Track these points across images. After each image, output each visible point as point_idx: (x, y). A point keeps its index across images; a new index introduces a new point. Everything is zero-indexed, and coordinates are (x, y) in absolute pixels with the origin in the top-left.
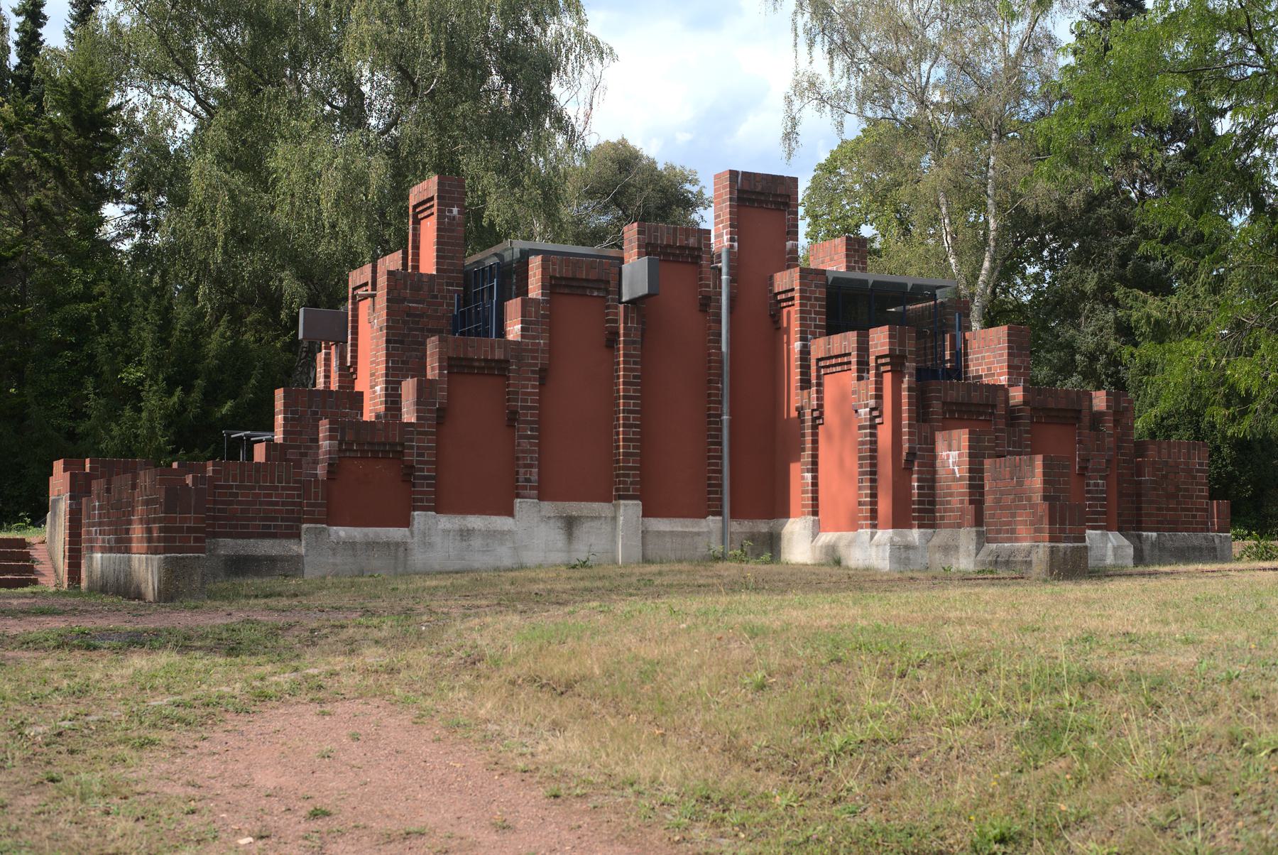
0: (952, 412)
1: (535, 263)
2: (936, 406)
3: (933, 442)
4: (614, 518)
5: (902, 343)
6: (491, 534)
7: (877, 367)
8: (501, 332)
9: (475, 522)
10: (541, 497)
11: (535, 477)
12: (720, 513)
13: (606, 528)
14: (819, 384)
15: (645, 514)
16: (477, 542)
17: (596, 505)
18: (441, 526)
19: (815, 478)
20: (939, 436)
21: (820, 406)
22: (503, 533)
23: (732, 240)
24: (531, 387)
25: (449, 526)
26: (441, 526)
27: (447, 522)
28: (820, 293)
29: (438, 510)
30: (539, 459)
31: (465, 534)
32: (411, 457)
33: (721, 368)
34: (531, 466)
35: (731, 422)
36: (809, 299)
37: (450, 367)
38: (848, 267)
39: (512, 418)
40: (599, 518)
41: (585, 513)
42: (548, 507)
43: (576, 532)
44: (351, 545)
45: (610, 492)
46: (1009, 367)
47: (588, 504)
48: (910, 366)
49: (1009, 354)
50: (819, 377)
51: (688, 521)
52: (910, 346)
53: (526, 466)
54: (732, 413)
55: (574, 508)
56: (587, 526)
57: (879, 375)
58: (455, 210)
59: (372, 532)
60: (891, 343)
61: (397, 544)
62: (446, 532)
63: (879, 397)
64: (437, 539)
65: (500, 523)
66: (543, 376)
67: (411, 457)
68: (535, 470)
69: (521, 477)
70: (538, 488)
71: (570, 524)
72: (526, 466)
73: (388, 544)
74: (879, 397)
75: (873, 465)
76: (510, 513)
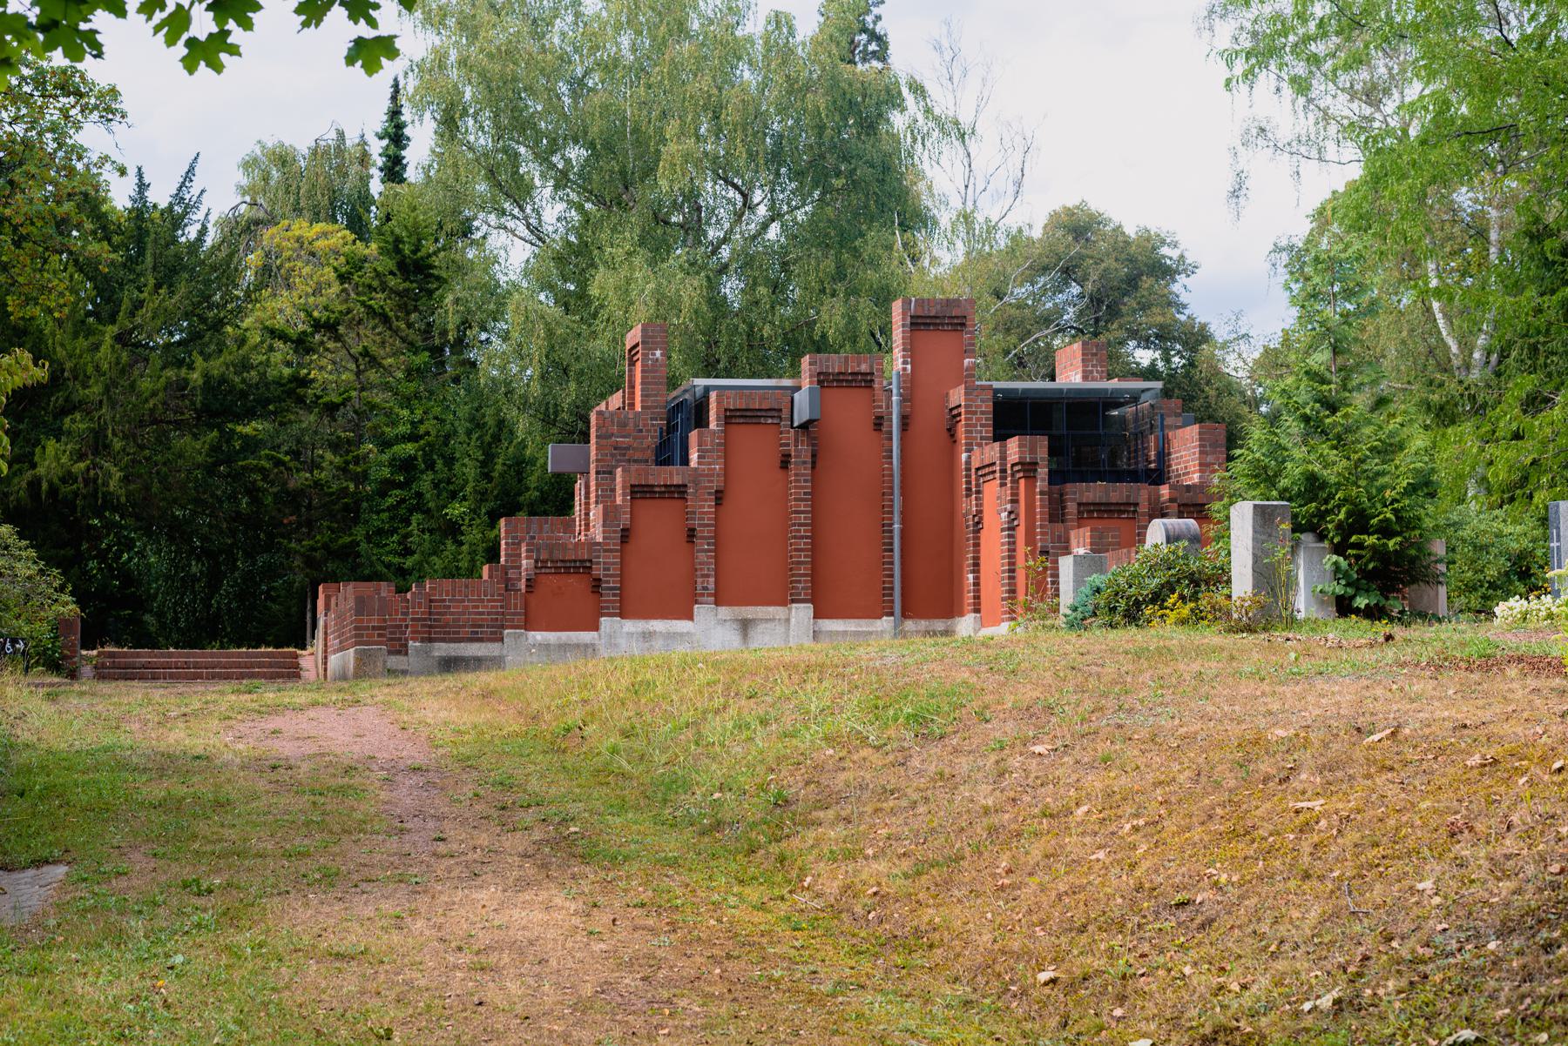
0: (1090, 512)
1: (713, 396)
2: (1072, 507)
3: (1068, 541)
4: (788, 620)
5: (1033, 451)
6: (670, 636)
7: (1013, 475)
8: (685, 461)
9: (658, 625)
10: (717, 603)
11: (712, 586)
12: (892, 614)
13: (780, 629)
14: (978, 492)
15: (818, 615)
16: (658, 643)
17: (771, 609)
18: (625, 629)
19: (977, 578)
20: (1073, 533)
21: (979, 512)
22: (681, 635)
23: (905, 363)
24: (708, 506)
25: (633, 629)
26: (625, 629)
27: (630, 626)
28: (988, 407)
29: (622, 615)
30: (716, 570)
31: (647, 636)
32: (598, 571)
33: (892, 481)
34: (708, 576)
35: (902, 531)
36: (975, 413)
37: (632, 493)
38: (1085, 378)
39: (691, 534)
40: (773, 620)
41: (760, 616)
42: (724, 612)
43: (751, 633)
44: (546, 647)
45: (786, 598)
46: (1201, 465)
47: (764, 609)
48: (1043, 472)
49: (1201, 452)
50: (978, 485)
51: (863, 622)
52: (1042, 453)
53: (703, 576)
54: (903, 522)
55: (749, 612)
56: (761, 627)
57: (1015, 482)
58: (658, 353)
59: (565, 636)
60: (1021, 452)
61: (586, 646)
62: (630, 634)
63: (1014, 501)
64: (622, 642)
65: (681, 626)
66: (719, 497)
67: (598, 571)
68: (712, 580)
69: (699, 586)
70: (715, 595)
71: (745, 626)
72: (703, 576)
73: (578, 646)
74: (1014, 501)
75: (1012, 564)
76: (690, 617)
